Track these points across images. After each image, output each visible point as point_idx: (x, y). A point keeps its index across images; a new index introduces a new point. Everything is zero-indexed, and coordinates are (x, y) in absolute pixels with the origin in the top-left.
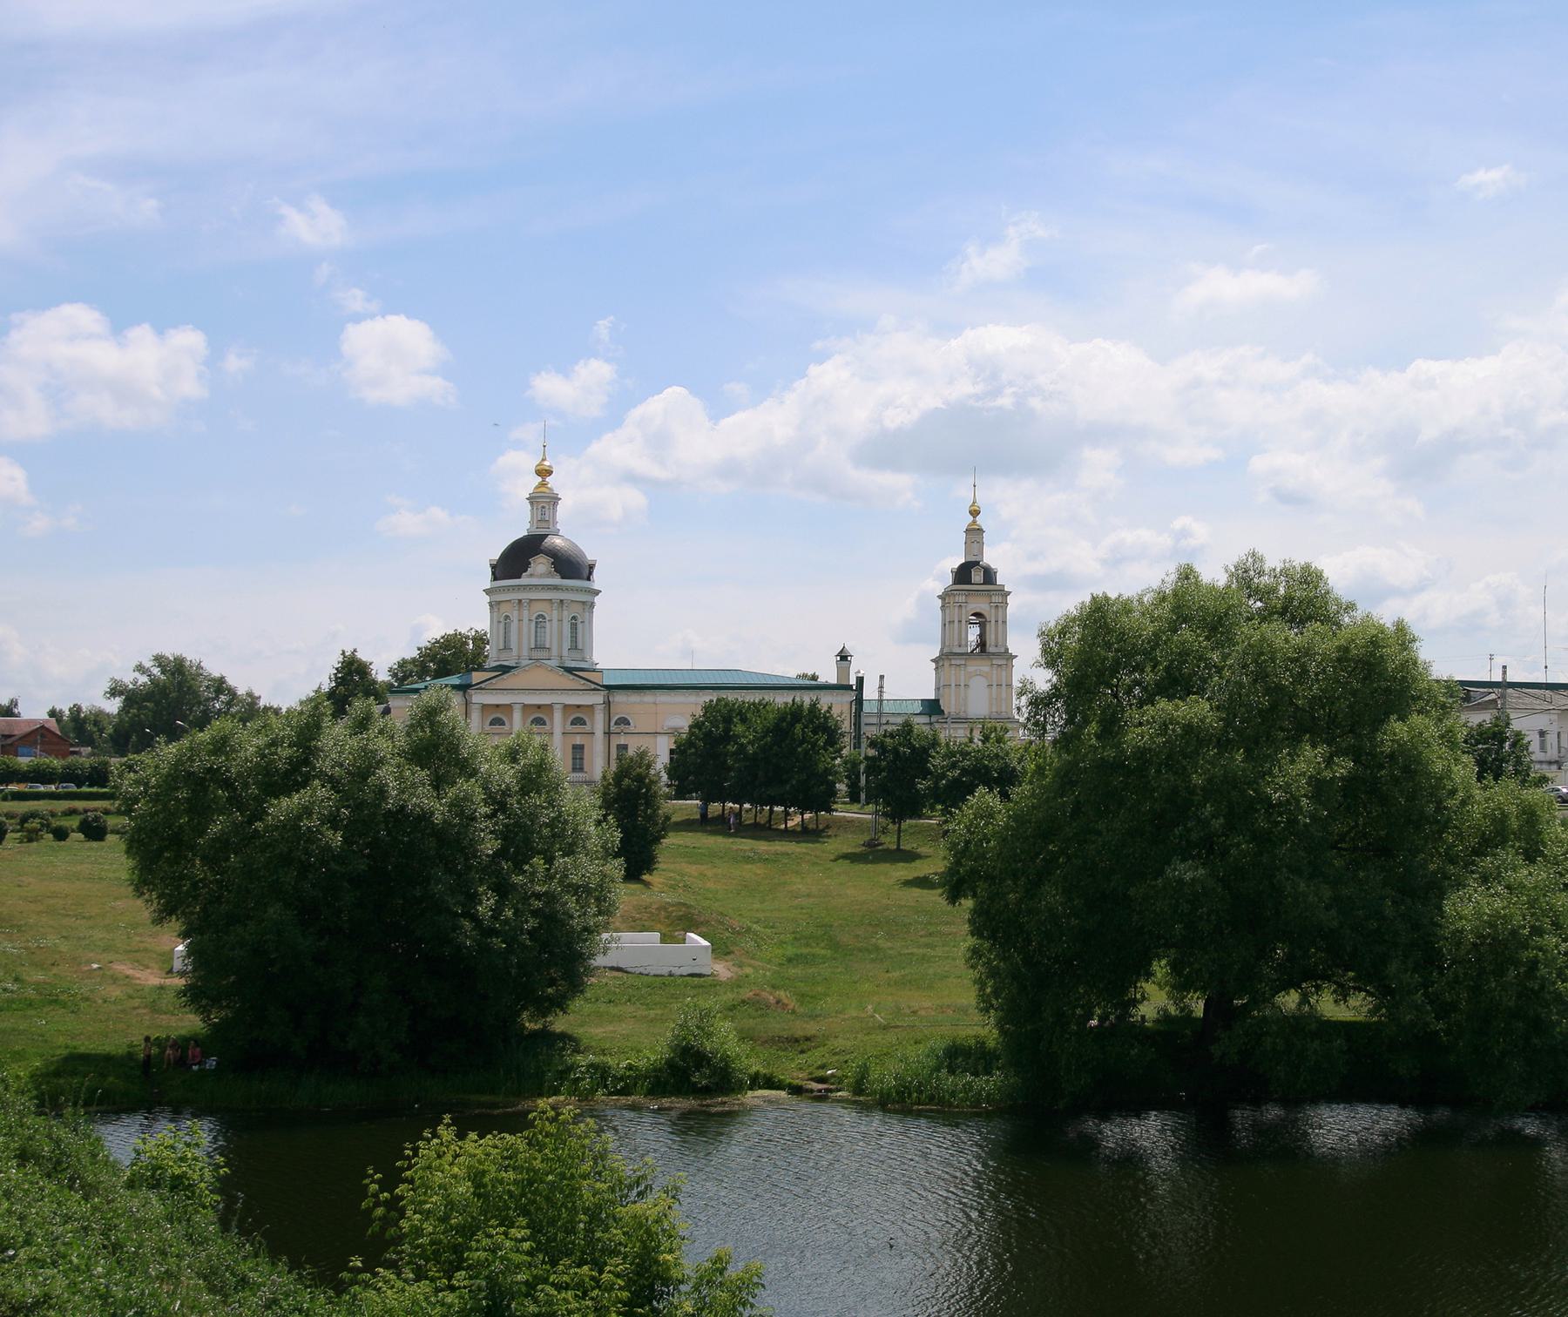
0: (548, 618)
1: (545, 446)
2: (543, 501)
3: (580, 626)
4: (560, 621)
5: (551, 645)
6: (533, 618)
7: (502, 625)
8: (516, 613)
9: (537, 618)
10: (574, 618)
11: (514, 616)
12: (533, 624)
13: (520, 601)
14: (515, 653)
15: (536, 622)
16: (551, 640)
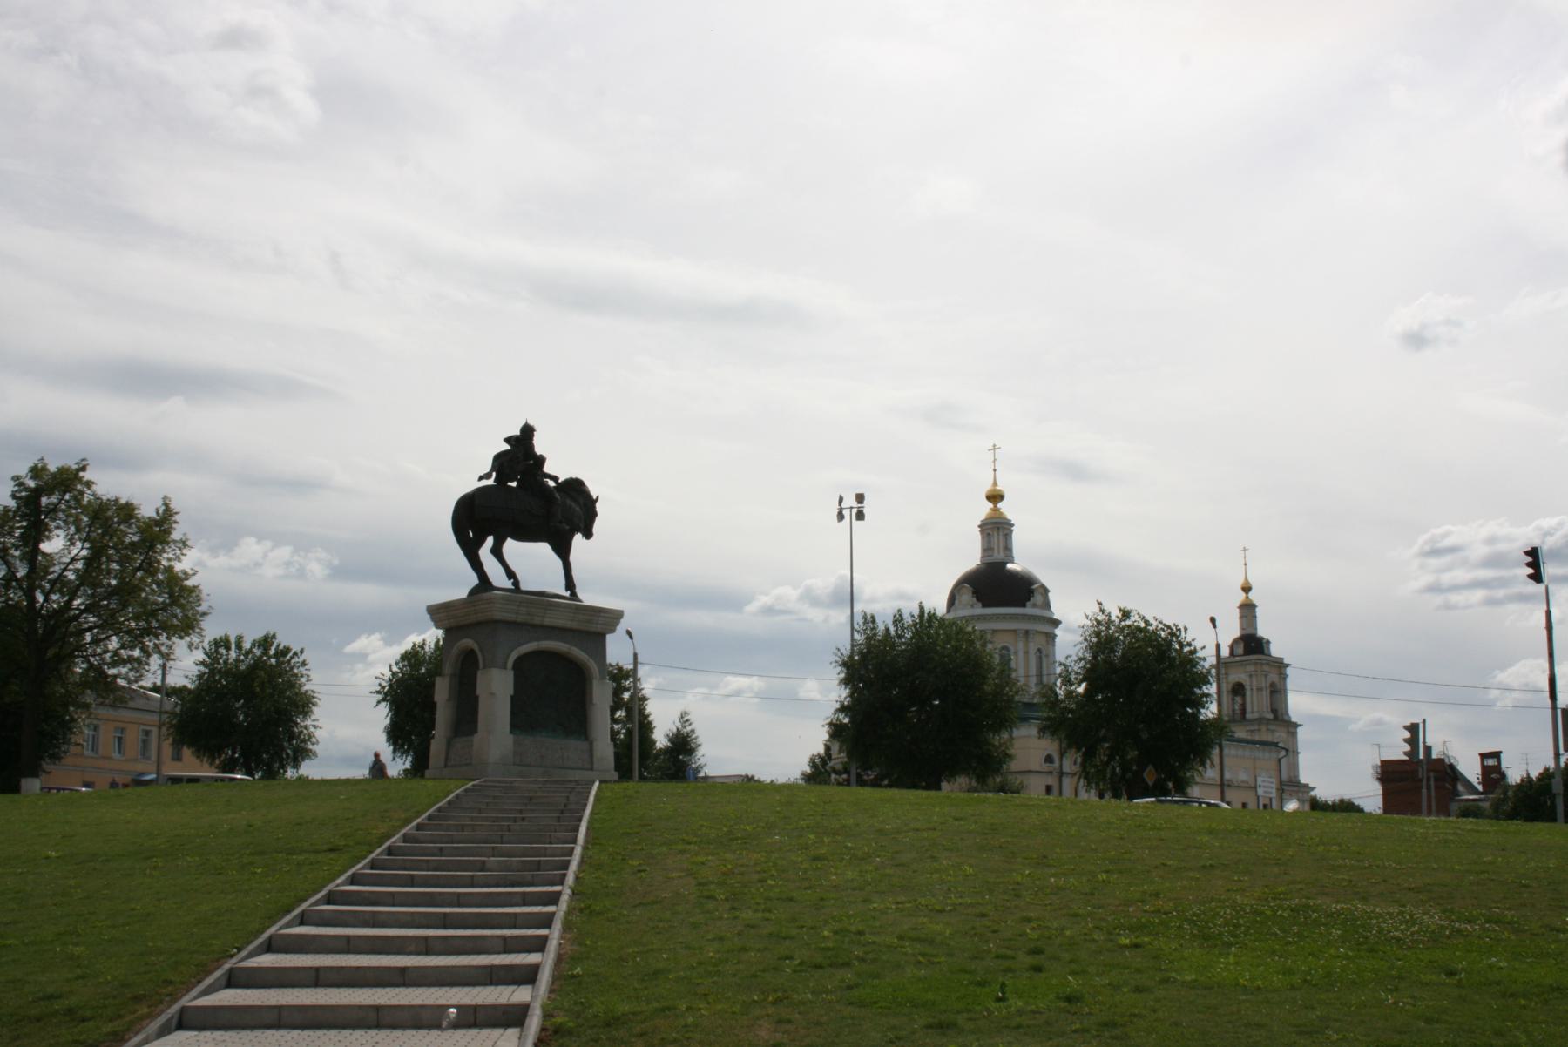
0: (1012, 649)
1: (995, 470)
2: (996, 530)
3: (1044, 659)
4: (1026, 653)
16: (1252, 703)
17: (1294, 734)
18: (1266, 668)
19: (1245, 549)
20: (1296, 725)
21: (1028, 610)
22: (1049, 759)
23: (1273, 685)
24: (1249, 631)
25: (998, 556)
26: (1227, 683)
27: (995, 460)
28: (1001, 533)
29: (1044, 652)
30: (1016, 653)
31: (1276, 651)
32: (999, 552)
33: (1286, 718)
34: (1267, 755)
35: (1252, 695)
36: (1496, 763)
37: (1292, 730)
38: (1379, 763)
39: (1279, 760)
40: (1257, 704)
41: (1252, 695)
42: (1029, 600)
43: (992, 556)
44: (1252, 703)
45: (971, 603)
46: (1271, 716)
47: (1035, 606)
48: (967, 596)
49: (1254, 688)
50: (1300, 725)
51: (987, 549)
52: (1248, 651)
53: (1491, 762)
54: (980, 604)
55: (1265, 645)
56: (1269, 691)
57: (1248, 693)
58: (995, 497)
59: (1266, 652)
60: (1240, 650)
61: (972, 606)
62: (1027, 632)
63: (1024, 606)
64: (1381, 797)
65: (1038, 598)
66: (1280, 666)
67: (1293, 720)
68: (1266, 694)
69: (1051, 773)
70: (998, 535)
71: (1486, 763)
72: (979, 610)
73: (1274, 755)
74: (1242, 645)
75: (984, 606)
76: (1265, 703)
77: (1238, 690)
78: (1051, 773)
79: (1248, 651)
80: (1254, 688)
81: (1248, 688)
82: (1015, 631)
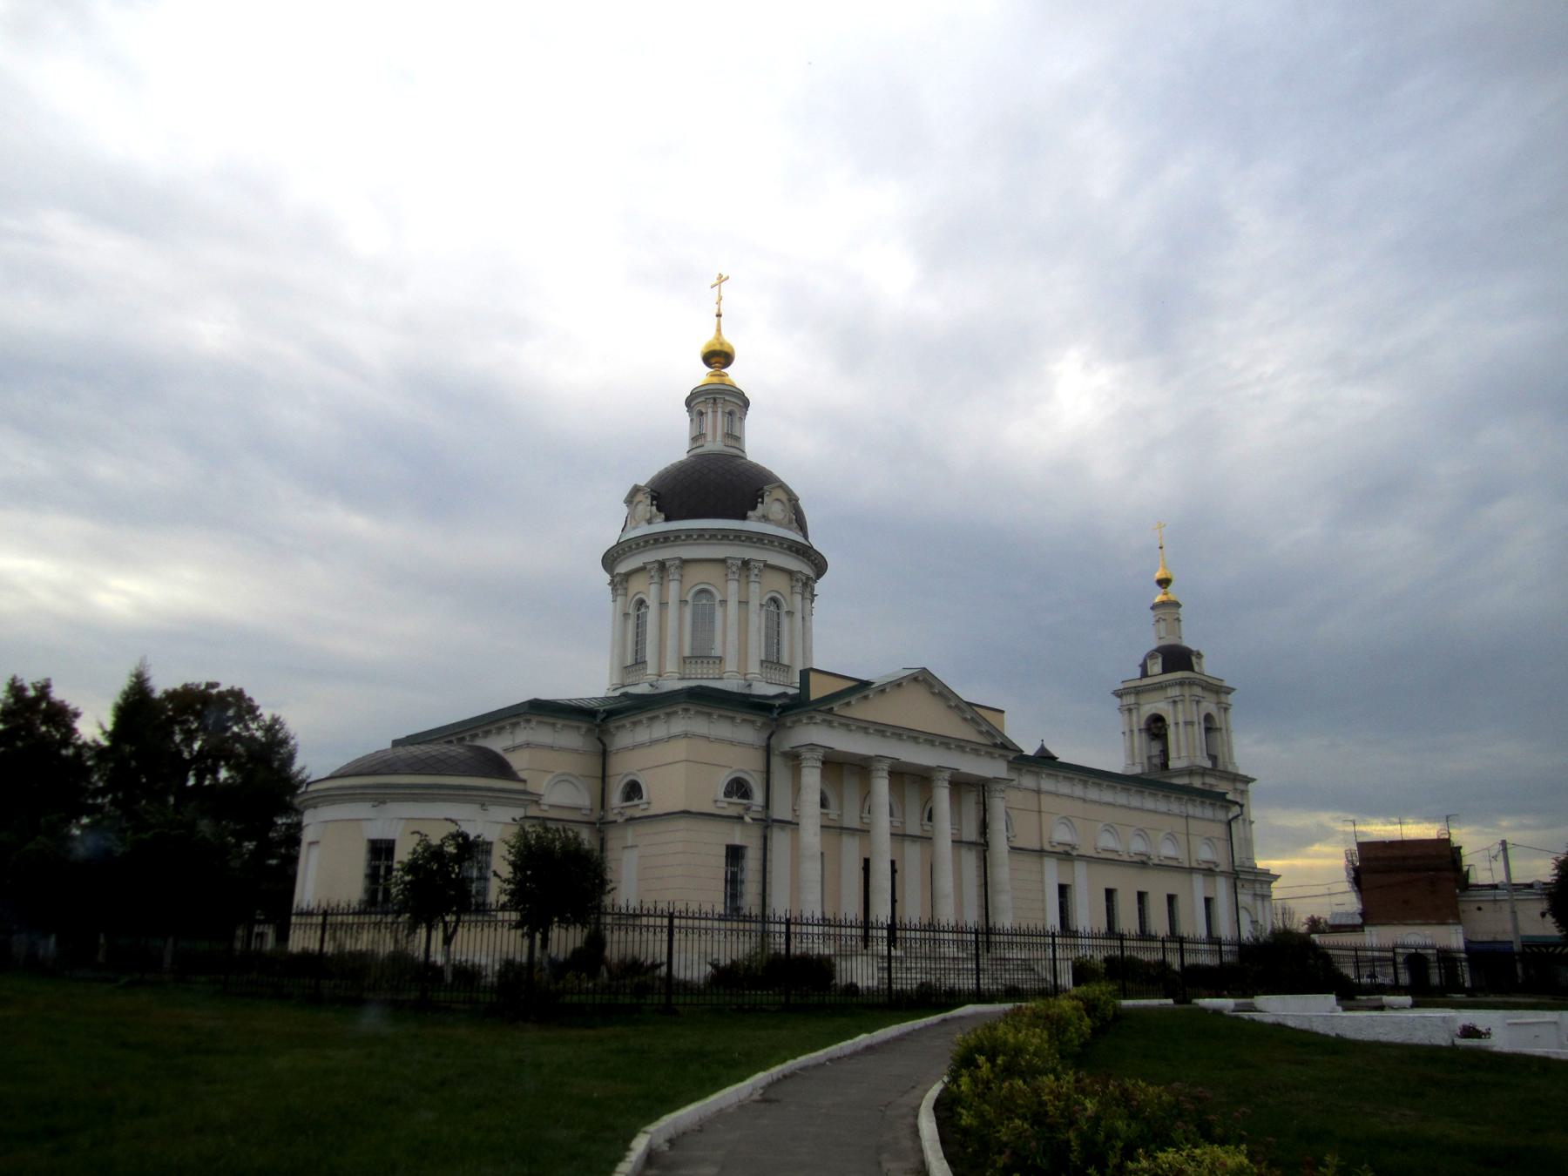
0: (718, 597)
3: (785, 621)
4: (743, 603)
5: (724, 651)
6: (689, 598)
7: (631, 624)
8: (654, 589)
10: (774, 600)
12: (688, 612)
13: (662, 566)
18: (1198, 691)
20: (1247, 780)
21: (751, 525)
22: (738, 788)
23: (1208, 718)
24: (1170, 640)
26: (1139, 716)
28: (720, 410)
29: (785, 608)
30: (724, 602)
31: (1209, 667)
33: (1230, 769)
34: (1209, 813)
35: (1177, 733)
37: (1240, 786)
38: (1355, 848)
39: (1229, 823)
40: (1185, 750)
41: (1177, 733)
42: (754, 508)
43: (702, 446)
44: (1178, 741)
45: (648, 516)
46: (1208, 764)
47: (765, 518)
48: (645, 507)
49: (1181, 724)
51: (697, 438)
54: (663, 516)
55: (1194, 659)
56: (1203, 726)
58: (718, 357)
59: (1196, 668)
60: (1156, 667)
61: (650, 522)
62: (746, 564)
63: (744, 517)
66: (1218, 690)
67: (1241, 772)
68: (1198, 731)
69: (740, 818)
70: (715, 412)
72: (661, 526)
73: (1221, 815)
74: (1160, 660)
75: (668, 519)
76: (1197, 742)
77: (1156, 728)
78: (740, 818)
80: (1181, 724)
81: (1170, 720)
82: (723, 561)
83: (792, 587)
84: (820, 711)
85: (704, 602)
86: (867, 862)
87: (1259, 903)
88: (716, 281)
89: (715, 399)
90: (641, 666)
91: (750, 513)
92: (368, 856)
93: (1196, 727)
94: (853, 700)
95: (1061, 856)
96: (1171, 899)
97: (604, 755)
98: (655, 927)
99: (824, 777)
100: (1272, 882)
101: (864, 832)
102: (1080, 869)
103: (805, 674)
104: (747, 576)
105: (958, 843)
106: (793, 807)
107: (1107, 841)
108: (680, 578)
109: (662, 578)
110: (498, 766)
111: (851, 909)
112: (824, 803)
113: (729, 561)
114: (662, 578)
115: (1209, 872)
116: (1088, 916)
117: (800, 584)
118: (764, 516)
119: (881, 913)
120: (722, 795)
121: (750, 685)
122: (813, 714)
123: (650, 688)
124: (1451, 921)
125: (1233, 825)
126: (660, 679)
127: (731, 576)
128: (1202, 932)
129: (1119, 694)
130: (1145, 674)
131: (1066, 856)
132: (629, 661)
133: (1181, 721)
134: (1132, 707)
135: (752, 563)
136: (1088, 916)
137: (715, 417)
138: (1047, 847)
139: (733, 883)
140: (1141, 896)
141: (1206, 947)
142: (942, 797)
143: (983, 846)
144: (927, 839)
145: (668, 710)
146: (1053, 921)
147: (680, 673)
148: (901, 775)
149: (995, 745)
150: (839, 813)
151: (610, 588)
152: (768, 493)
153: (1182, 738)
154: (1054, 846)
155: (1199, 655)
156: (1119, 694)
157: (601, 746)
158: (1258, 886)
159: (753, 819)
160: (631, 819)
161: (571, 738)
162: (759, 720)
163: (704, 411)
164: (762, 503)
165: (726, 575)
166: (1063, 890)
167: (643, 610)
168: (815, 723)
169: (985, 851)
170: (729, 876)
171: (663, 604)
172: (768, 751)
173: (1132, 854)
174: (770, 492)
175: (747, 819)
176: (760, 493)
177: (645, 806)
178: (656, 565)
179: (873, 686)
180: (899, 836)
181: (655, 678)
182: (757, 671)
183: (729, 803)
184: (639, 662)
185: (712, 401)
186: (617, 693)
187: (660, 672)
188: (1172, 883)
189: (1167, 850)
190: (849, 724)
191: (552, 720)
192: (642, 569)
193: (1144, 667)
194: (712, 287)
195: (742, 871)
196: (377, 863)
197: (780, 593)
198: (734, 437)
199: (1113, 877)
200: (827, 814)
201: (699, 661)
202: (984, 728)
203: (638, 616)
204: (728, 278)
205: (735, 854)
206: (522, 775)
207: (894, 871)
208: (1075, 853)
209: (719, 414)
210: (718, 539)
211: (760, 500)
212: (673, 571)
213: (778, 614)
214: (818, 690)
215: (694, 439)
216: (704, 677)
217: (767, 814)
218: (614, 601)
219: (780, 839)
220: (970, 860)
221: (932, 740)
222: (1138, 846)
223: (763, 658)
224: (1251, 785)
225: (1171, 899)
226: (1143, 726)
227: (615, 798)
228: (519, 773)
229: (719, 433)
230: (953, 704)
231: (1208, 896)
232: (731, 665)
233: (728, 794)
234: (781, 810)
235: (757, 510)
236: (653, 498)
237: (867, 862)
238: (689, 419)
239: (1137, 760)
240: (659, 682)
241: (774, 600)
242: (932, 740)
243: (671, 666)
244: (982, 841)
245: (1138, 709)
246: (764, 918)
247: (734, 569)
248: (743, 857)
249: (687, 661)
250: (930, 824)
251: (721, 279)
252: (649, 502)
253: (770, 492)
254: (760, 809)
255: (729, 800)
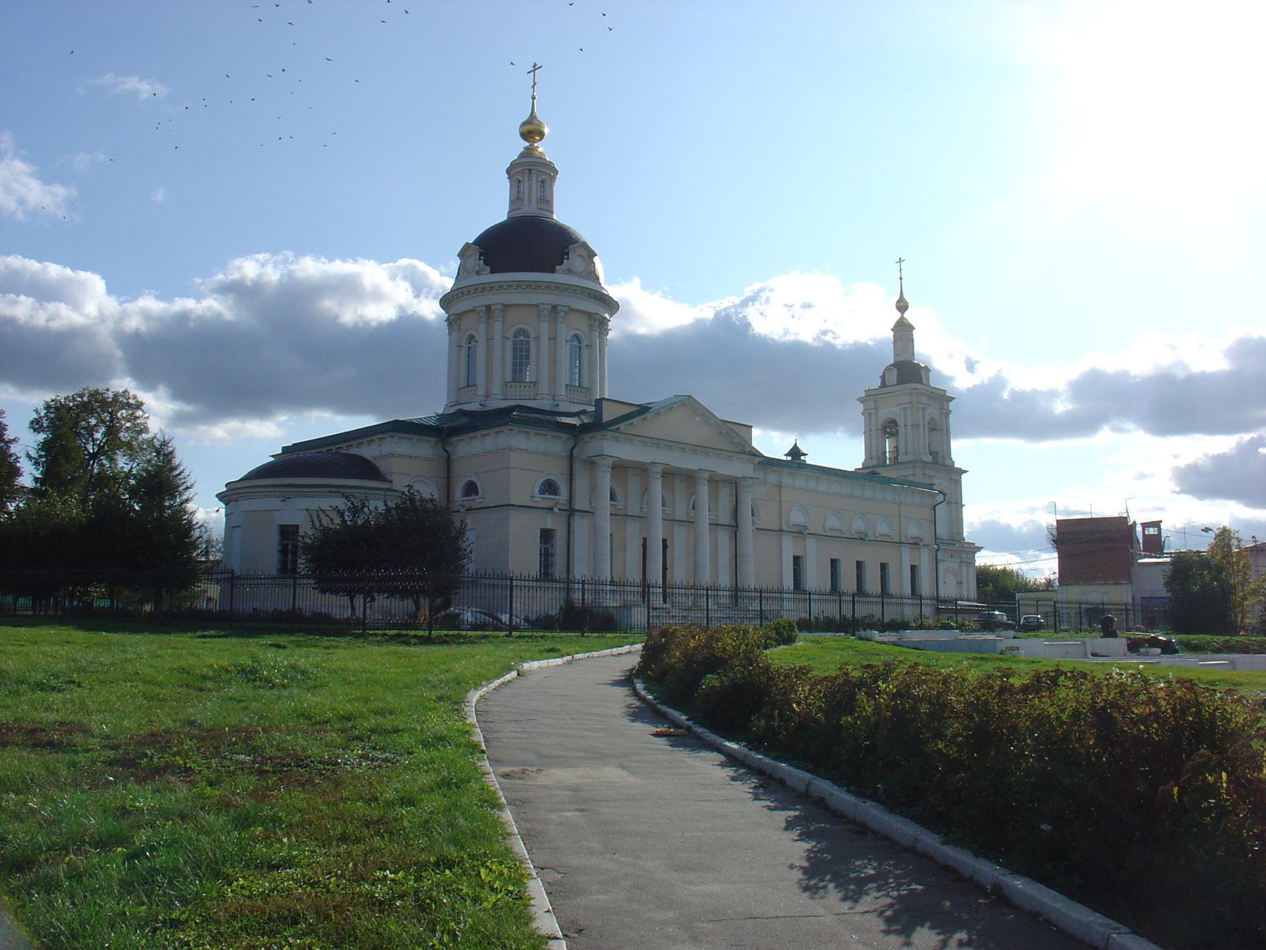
0: (532, 335)
1: (534, 98)
3: (585, 352)
4: (553, 338)
6: (510, 334)
7: (464, 352)
8: (482, 327)
9: (514, 337)
11: (480, 331)
13: (488, 308)
14: (481, 390)
15: (515, 343)
17: (958, 483)
18: (925, 400)
19: (900, 261)
21: (559, 277)
22: (550, 487)
25: (529, 209)
27: (535, 84)
28: (534, 179)
29: (585, 342)
30: (537, 338)
32: (530, 206)
33: (947, 462)
36: (1156, 533)
37: (954, 476)
39: (935, 506)
42: (561, 263)
45: (477, 269)
46: (929, 459)
47: (569, 271)
48: (475, 261)
50: (966, 472)
51: (516, 200)
52: (901, 381)
53: (1152, 531)
55: (923, 373)
57: (901, 431)
58: (531, 131)
59: (924, 381)
60: (893, 378)
61: (478, 273)
62: (554, 308)
63: (553, 271)
64: (1057, 560)
65: (575, 261)
67: (956, 465)
69: (551, 509)
70: (530, 180)
71: (1147, 533)
74: (896, 372)
75: (492, 272)
79: (901, 381)
81: (901, 422)
83: (590, 325)
84: (610, 430)
85: (521, 338)
86: (645, 539)
87: (964, 569)
88: (533, 69)
89: (530, 171)
90: (472, 388)
91: (558, 267)
92: (280, 537)
93: (921, 429)
94: (635, 420)
95: (795, 534)
96: (883, 567)
97: (449, 461)
98: (521, 587)
99: (612, 476)
100: (976, 552)
101: (643, 518)
102: (811, 544)
103: (599, 403)
104: (555, 318)
105: (715, 525)
106: (589, 500)
107: (833, 522)
108: (501, 319)
109: (488, 319)
110: (368, 470)
111: (634, 575)
112: (613, 498)
113: (542, 306)
114: (488, 319)
115: (916, 544)
116: (816, 579)
117: (597, 323)
118: (569, 270)
119: (656, 576)
120: (538, 493)
121: (557, 405)
122: (605, 432)
123: (481, 407)
124: (1124, 582)
125: (937, 507)
126: (488, 399)
127: (542, 318)
128: (907, 590)
129: (861, 400)
130: (883, 385)
131: (800, 532)
132: (463, 383)
133: (909, 423)
134: (873, 411)
135: (560, 308)
136: (816, 579)
137: (530, 187)
138: (784, 528)
139: (546, 558)
140: (859, 565)
141: (909, 601)
142: (704, 491)
143: (735, 528)
144: (690, 523)
145: (497, 430)
146: (789, 583)
147: (503, 395)
148: (670, 474)
149: (744, 453)
150: (625, 504)
151: (446, 323)
152: (572, 251)
153: (910, 438)
154: (790, 527)
155: (927, 369)
156: (861, 400)
157: (446, 455)
158: (964, 556)
159: (559, 510)
160: (470, 509)
161: (424, 449)
162: (564, 436)
163: (521, 180)
164: (568, 259)
165: (539, 317)
166: (797, 560)
167: (473, 344)
168: (606, 439)
169: (736, 532)
170: (543, 550)
171: (489, 339)
172: (571, 458)
173: (853, 533)
174: (574, 250)
175: (556, 510)
176: (566, 250)
177: (481, 500)
178: (484, 308)
179: (652, 410)
180: (670, 521)
181: (483, 398)
182: (564, 394)
183: (542, 498)
184: (470, 384)
185: (528, 171)
186: (453, 410)
187: (487, 392)
188: (886, 555)
189: (882, 528)
190: (630, 438)
191: (409, 436)
192: (473, 310)
193: (883, 378)
194: (529, 73)
195: (552, 547)
196: (286, 542)
197: (583, 332)
198: (546, 201)
199: (836, 550)
200: (615, 505)
201: (518, 386)
202: (736, 440)
203: (469, 347)
204: (541, 67)
205: (547, 535)
206: (388, 477)
207: (665, 546)
208: (806, 532)
209: (534, 185)
210: (532, 289)
211: (566, 257)
212: (497, 314)
213: (580, 347)
214: (608, 414)
215: (512, 203)
216: (520, 397)
217: (570, 505)
218: (450, 334)
219: (580, 524)
220: (724, 537)
221: (696, 449)
222: (858, 525)
223: (568, 383)
224: (964, 476)
225: (883, 567)
226: (880, 427)
227: (458, 494)
228: (385, 475)
229: (534, 198)
230: (712, 422)
231: (913, 564)
232: (544, 388)
233: (542, 492)
234: (580, 504)
235: (563, 265)
236: (481, 254)
237: (645, 539)
238: (509, 185)
239: (874, 454)
240: (488, 402)
241: (576, 336)
242: (696, 449)
243: (497, 389)
244: (735, 524)
245: (876, 413)
246: (569, 581)
247: (545, 312)
248: (553, 536)
249: (509, 385)
250: (693, 511)
251: (536, 68)
252: (478, 257)
253: (574, 250)
254: (565, 502)
255: (542, 496)
